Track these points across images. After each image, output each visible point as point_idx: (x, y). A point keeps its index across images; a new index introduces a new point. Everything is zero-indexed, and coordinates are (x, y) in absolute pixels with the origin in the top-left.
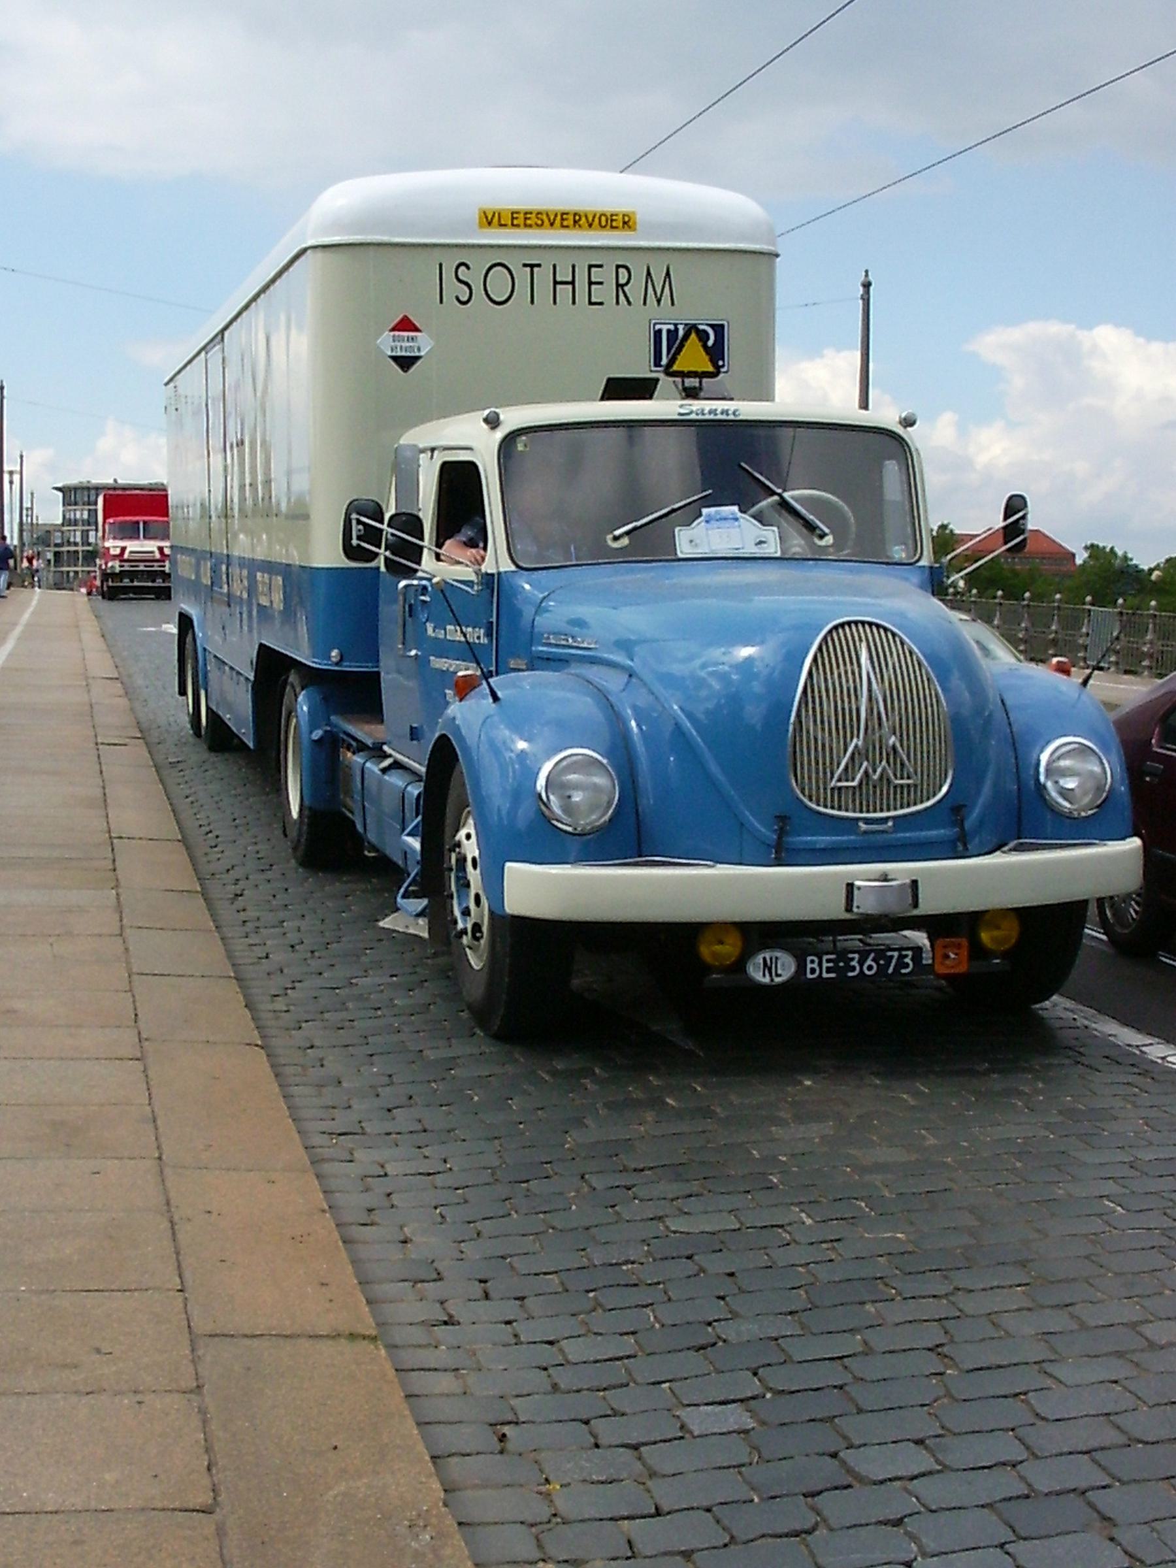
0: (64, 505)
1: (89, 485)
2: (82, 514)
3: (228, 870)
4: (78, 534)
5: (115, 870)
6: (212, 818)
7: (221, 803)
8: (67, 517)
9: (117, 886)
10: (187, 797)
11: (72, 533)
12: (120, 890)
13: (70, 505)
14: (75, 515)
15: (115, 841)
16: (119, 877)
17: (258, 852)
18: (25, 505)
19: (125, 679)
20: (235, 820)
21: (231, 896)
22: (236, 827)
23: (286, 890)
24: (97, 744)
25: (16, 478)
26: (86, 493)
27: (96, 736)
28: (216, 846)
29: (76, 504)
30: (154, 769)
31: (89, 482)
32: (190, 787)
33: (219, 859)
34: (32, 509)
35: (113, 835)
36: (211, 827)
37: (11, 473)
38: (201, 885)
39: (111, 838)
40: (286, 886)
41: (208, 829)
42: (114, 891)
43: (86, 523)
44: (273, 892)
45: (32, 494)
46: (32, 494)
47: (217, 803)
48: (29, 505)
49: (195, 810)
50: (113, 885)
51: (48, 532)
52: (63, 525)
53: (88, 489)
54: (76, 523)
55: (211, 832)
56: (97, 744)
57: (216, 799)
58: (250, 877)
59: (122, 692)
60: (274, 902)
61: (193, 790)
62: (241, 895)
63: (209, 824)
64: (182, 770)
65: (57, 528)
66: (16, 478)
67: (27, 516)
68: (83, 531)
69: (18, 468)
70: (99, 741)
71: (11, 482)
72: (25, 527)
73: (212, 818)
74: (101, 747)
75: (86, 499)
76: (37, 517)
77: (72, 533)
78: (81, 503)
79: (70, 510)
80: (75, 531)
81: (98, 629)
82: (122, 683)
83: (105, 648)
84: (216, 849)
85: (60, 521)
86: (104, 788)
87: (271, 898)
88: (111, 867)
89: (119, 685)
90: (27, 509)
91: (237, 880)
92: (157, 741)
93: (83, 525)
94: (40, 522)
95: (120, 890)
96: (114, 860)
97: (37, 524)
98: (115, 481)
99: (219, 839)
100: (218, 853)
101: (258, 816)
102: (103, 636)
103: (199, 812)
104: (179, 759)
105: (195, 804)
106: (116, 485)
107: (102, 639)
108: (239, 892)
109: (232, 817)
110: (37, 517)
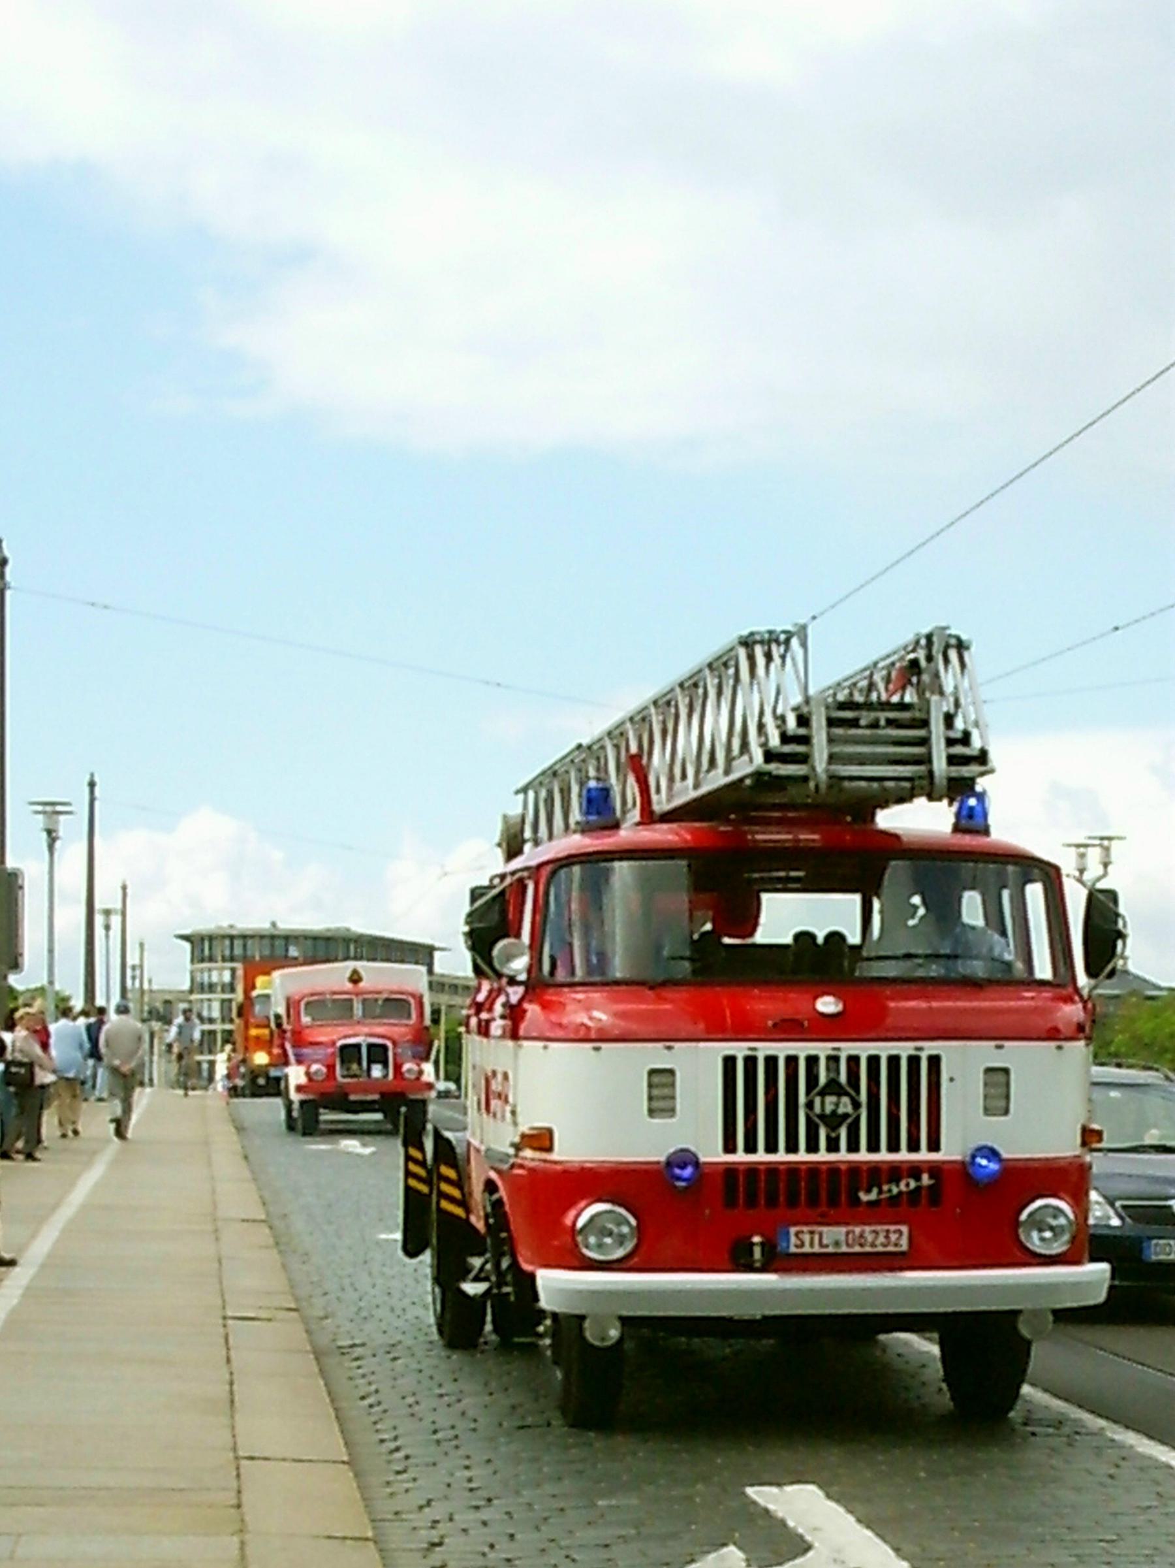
0: (192, 961)
1: (234, 932)
2: (220, 975)
3: (421, 1508)
4: (216, 1006)
5: (239, 1506)
6: (400, 1431)
7: (416, 1408)
8: (198, 979)
9: (241, 1531)
10: (363, 1398)
11: (206, 1005)
12: (247, 1537)
13: (202, 960)
14: (210, 977)
15: (244, 1463)
16: (247, 1518)
17: (470, 1480)
18: (130, 962)
19: (277, 1223)
20: (435, 1432)
21: (425, 1545)
22: (438, 1442)
23: (512, 1536)
24: (225, 1318)
25: (116, 920)
26: (227, 942)
27: (224, 1308)
28: (405, 1471)
29: (211, 959)
30: (312, 1356)
31: (231, 927)
32: (370, 1384)
33: (407, 1491)
34: (141, 966)
35: (241, 1453)
36: (398, 1443)
37: (107, 913)
38: (374, 1528)
39: (237, 1458)
40: (512, 1531)
41: (393, 1445)
42: (236, 1539)
43: (228, 989)
44: (490, 1540)
45: (142, 945)
46: (142, 945)
47: (410, 1406)
48: (137, 962)
49: (373, 1419)
50: (237, 1526)
51: (167, 1002)
52: (191, 991)
53: (232, 938)
54: (211, 988)
55: (397, 1449)
56: (225, 1318)
57: (410, 1400)
58: (456, 1517)
59: (271, 1241)
60: (492, 1555)
61: (373, 1388)
62: (440, 1544)
63: (396, 1438)
64: (357, 1359)
65: (181, 996)
66: (116, 920)
67: (134, 978)
68: (223, 1001)
69: (119, 906)
70: (230, 1314)
71: (107, 928)
72: (130, 995)
73: (400, 1431)
74: (230, 1322)
75: (227, 953)
76: (150, 981)
77: (206, 1005)
78: (220, 958)
79: (202, 971)
80: (209, 1000)
81: (239, 1147)
82: (271, 1228)
83: (247, 1174)
84: (405, 1476)
85: (186, 986)
86: (231, 1384)
87: (486, 1549)
88: (234, 1502)
89: (267, 1231)
90: (134, 968)
91: (436, 1522)
92: (321, 1314)
93: (223, 991)
94: (155, 987)
95: (247, 1537)
96: (239, 1492)
97: (151, 991)
98: (274, 924)
99: (411, 1461)
100: (408, 1481)
101: (472, 1425)
102: (246, 1157)
103: (381, 1419)
104: (357, 1341)
105: (376, 1409)
106: (276, 933)
107: (243, 1163)
108: (436, 1540)
109: (433, 1427)
110: (150, 981)
